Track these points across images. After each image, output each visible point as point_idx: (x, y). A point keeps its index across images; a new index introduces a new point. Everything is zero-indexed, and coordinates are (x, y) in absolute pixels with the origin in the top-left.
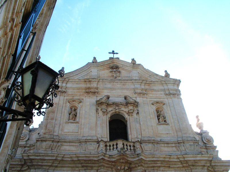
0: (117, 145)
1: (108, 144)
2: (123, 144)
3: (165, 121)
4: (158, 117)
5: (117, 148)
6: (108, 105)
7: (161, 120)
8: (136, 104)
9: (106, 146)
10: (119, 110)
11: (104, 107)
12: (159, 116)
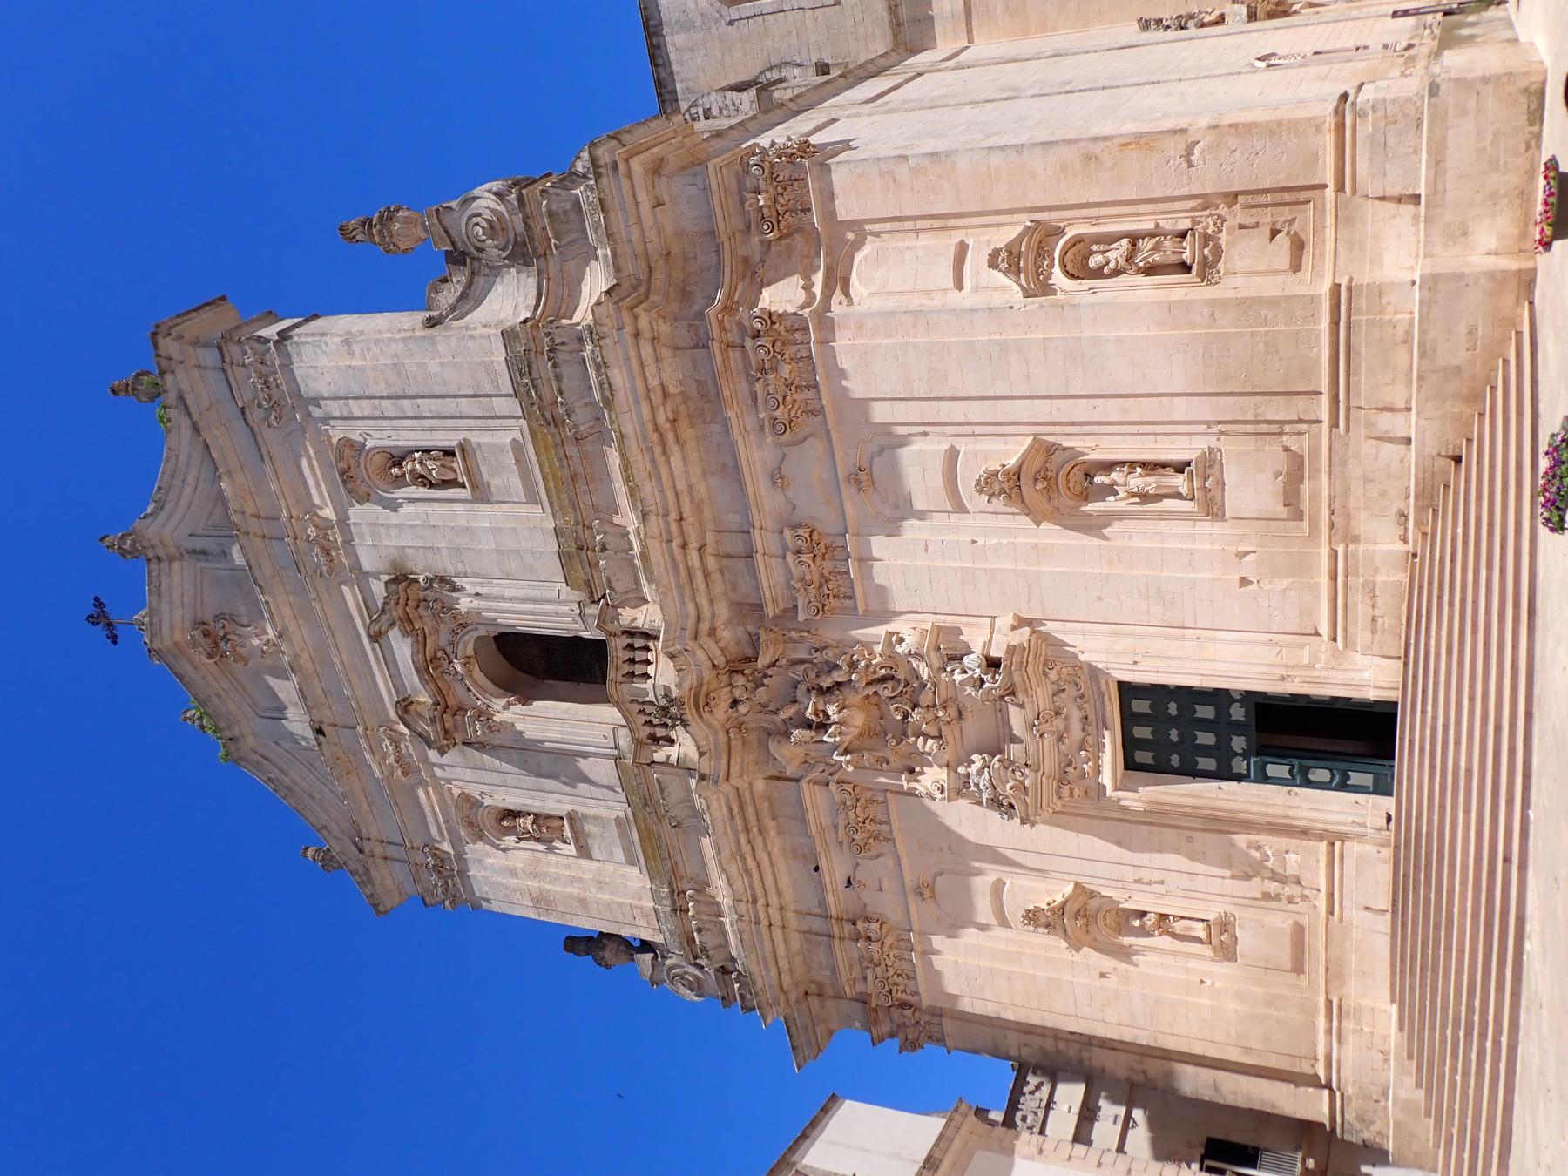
3: (449, 453)
10: (452, 656)
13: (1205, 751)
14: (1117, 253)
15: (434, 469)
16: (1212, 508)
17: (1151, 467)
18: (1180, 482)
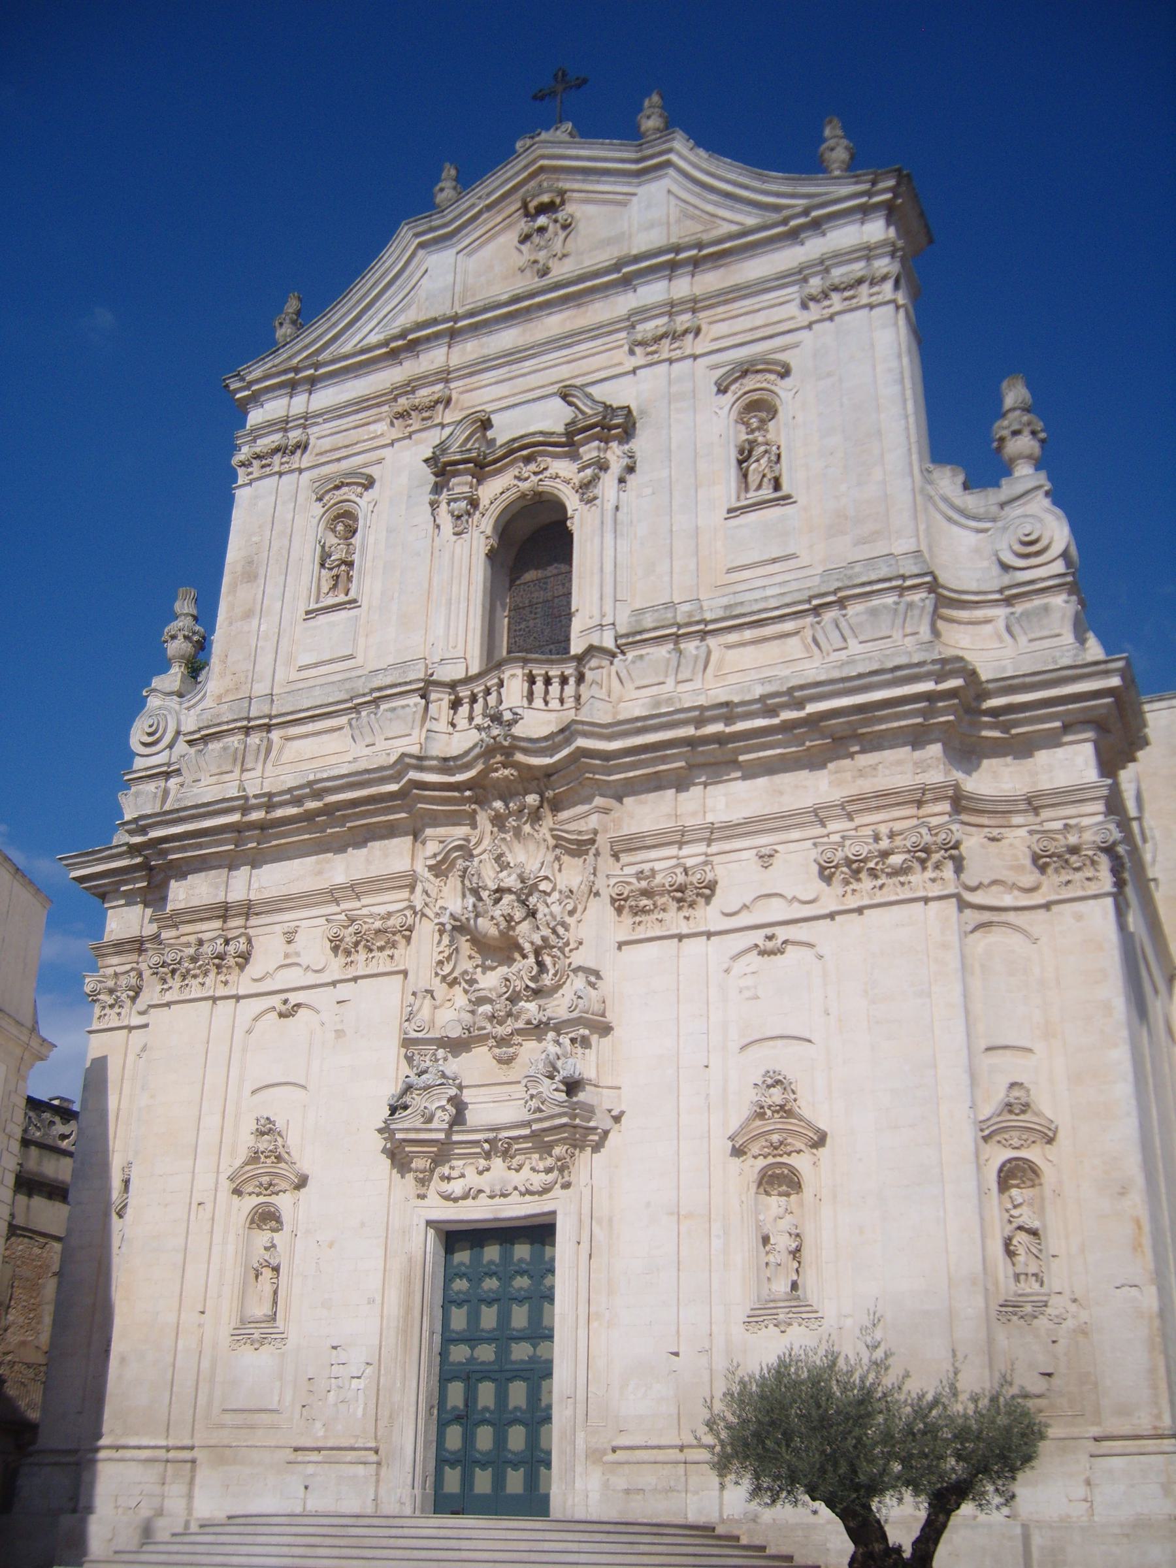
0: (501, 684)
1: (464, 692)
2: (532, 680)
4: (740, 462)
6: (481, 468)
7: (753, 479)
9: (455, 705)
10: (541, 476)
11: (461, 484)
13: (474, 1318)
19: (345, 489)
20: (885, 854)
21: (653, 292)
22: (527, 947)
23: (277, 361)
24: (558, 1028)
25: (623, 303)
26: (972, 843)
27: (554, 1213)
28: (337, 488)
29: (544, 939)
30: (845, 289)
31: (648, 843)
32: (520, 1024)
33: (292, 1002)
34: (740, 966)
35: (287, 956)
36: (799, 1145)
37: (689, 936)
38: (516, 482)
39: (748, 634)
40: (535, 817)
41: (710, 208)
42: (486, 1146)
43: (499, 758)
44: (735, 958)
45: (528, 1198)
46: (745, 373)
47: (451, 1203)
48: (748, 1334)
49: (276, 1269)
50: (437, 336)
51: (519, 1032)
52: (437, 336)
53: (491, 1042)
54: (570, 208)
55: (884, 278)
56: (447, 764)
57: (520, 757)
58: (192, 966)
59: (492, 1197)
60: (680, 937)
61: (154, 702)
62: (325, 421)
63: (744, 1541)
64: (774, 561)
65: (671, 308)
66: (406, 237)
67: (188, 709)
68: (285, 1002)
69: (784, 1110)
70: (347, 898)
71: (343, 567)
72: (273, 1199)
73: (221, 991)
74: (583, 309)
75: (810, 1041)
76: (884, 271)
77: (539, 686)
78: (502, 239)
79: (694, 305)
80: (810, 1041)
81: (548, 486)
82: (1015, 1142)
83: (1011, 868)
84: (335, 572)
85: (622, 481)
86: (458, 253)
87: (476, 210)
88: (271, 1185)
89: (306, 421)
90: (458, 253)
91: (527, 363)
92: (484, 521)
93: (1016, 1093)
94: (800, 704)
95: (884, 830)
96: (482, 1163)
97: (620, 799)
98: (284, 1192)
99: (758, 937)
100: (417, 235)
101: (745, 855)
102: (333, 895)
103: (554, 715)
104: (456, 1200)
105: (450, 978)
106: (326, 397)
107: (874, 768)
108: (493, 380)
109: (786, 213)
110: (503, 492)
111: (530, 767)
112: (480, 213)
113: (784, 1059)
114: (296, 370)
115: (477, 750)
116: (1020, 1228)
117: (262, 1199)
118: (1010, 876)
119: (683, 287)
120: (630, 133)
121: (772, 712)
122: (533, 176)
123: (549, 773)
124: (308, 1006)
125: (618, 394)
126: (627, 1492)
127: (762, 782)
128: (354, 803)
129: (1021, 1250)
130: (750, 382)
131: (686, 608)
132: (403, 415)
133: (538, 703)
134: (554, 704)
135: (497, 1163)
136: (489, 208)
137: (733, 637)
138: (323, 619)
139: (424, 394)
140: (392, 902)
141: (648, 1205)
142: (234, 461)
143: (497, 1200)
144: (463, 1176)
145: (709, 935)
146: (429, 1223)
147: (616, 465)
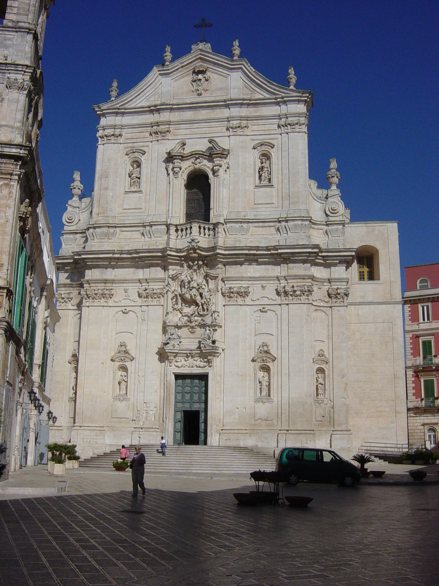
0: (191, 228)
1: (179, 228)
2: (200, 228)
3: (270, 180)
4: (259, 172)
5: (191, 233)
6: (183, 158)
8: (224, 154)
9: (177, 230)
10: (201, 164)
12: (262, 171)
14: (321, 380)
15: (265, 175)
16: (257, 401)
17: (269, 386)
18: (264, 393)
19: (136, 154)
20: (295, 291)
21: (235, 111)
22: (200, 304)
23: (112, 104)
24: (209, 326)
25: (225, 113)
26: (315, 288)
27: (208, 373)
28: (134, 152)
29: (205, 302)
30: (292, 125)
31: (233, 279)
32: (197, 323)
33: (128, 310)
34: (255, 315)
35: (125, 296)
36: (270, 361)
37: (243, 305)
38: (192, 164)
39: (261, 224)
40: (199, 267)
41: (253, 87)
42: (189, 355)
43: (192, 251)
44: (255, 312)
45: (199, 368)
46: (262, 145)
47: (178, 368)
48: (255, 404)
49: (127, 382)
50: (167, 109)
51: (197, 325)
52: (167, 109)
53: (189, 327)
54: (208, 74)
55: (303, 124)
56: (178, 251)
57: (198, 251)
58: (96, 296)
59: (189, 367)
60: (241, 305)
61: (69, 209)
62: (128, 128)
63: (255, 451)
64: (268, 204)
65: (241, 118)
66: (155, 71)
67: (82, 213)
68: (126, 310)
69: (267, 352)
70: (144, 282)
71: (136, 179)
72: (124, 363)
73: (106, 304)
74: (213, 111)
75: (273, 335)
76: (303, 122)
77: (202, 229)
78: (186, 78)
79: (247, 118)
80: (273, 335)
81: (203, 168)
82: (320, 363)
83: (323, 296)
84: (134, 180)
85: (226, 171)
86: (172, 79)
87: (178, 67)
88: (124, 359)
89: (122, 127)
90: (172, 79)
91: (196, 125)
92: (183, 175)
93: (321, 352)
94: (277, 250)
95: (295, 285)
96: (187, 359)
97: (225, 266)
98: (128, 361)
99: (261, 307)
100: (159, 71)
101: (258, 285)
102: (140, 281)
103: (207, 239)
104: (179, 367)
105: (177, 309)
106: (127, 120)
107: (293, 268)
108: (184, 128)
109: (277, 96)
110: (189, 167)
111: (201, 254)
112: (180, 68)
113: (266, 339)
114: (119, 109)
115: (187, 248)
116: (320, 383)
117: (121, 363)
118: (323, 298)
119: (244, 111)
120: (230, 55)
121: (269, 250)
122: (197, 59)
123: (206, 256)
124: (132, 311)
125: (224, 143)
126: (226, 439)
127: (263, 266)
128: (148, 257)
129: (319, 388)
130: (264, 148)
131: (244, 213)
132: (156, 133)
133: (202, 235)
134: (207, 236)
135: (190, 358)
136: (182, 67)
137: (257, 224)
138: (131, 195)
139: (162, 128)
140: (160, 285)
141: (231, 372)
142: (97, 135)
143: (190, 368)
144: (181, 361)
145: (248, 305)
146: (173, 373)
147: (224, 167)
